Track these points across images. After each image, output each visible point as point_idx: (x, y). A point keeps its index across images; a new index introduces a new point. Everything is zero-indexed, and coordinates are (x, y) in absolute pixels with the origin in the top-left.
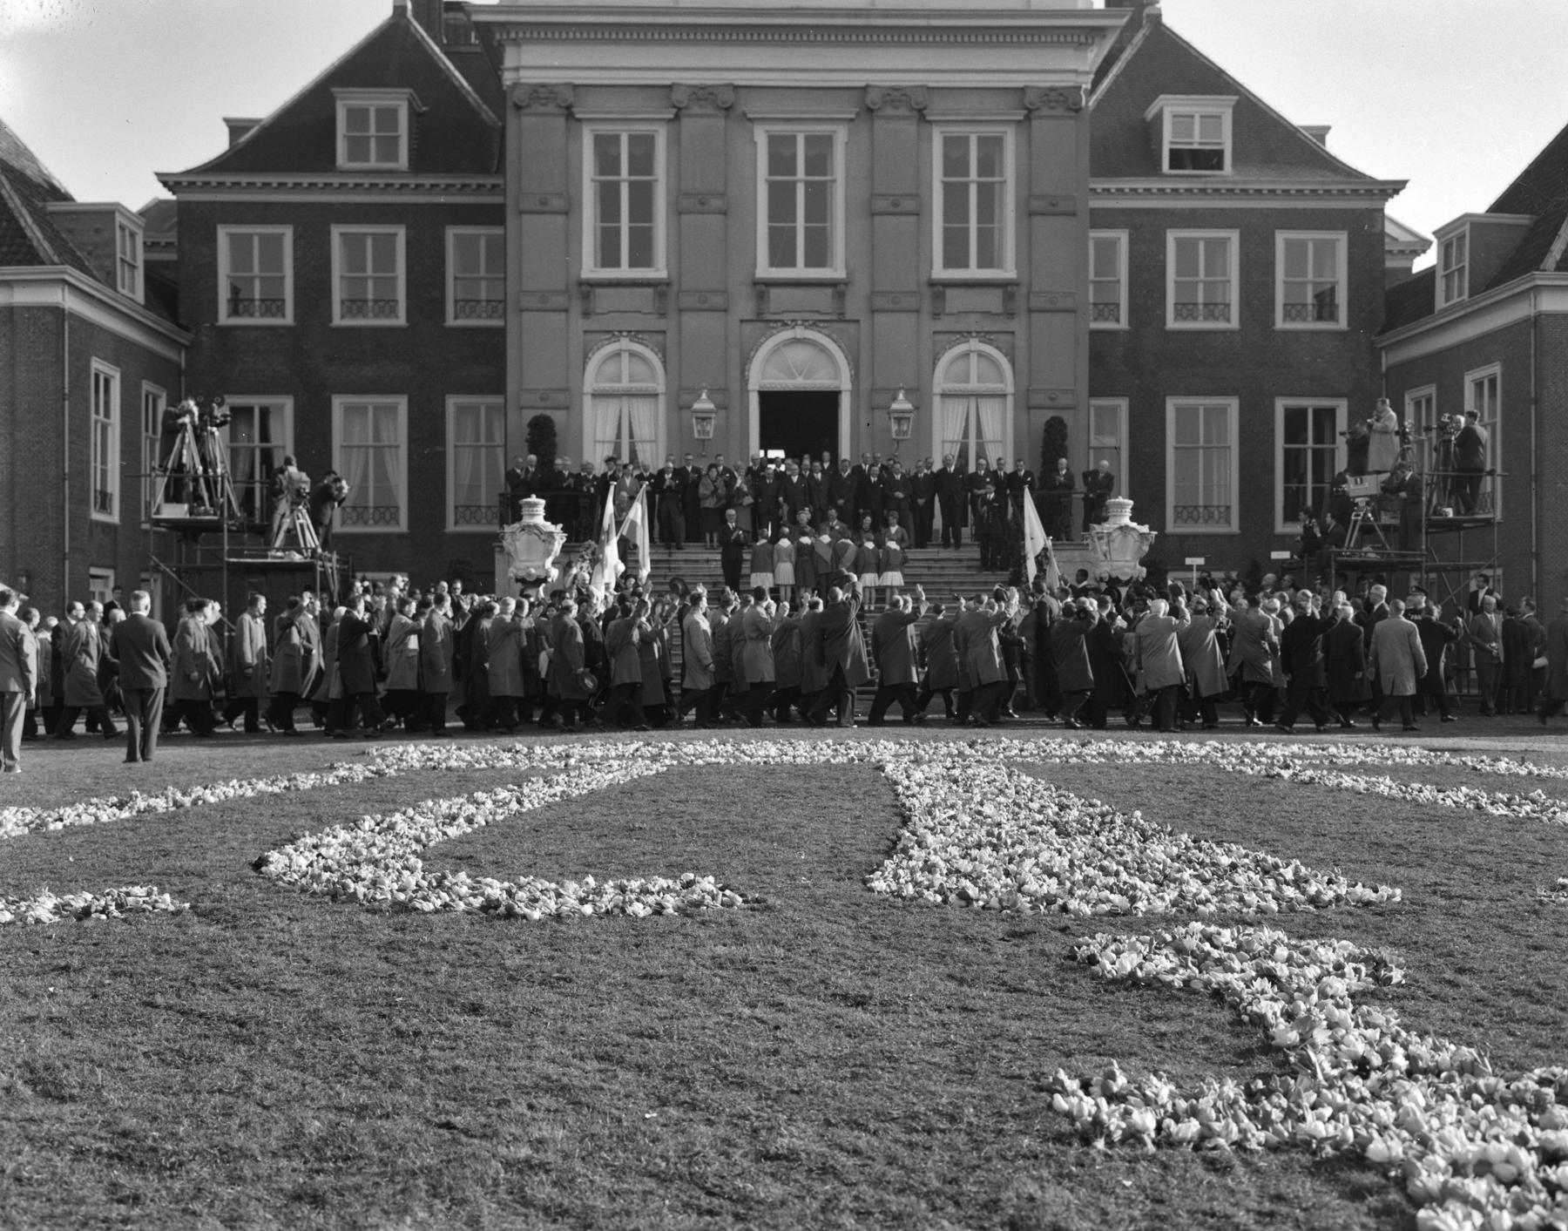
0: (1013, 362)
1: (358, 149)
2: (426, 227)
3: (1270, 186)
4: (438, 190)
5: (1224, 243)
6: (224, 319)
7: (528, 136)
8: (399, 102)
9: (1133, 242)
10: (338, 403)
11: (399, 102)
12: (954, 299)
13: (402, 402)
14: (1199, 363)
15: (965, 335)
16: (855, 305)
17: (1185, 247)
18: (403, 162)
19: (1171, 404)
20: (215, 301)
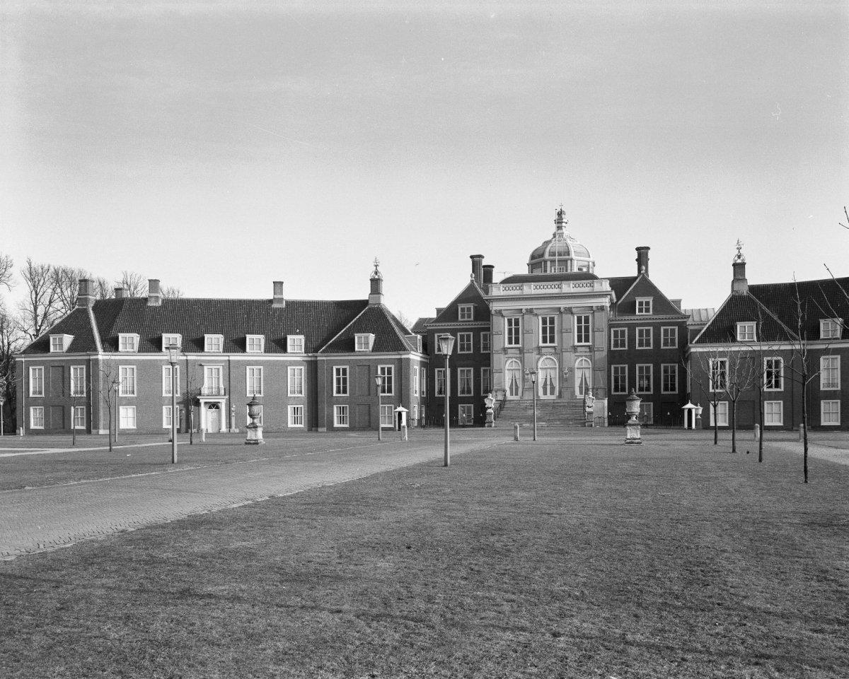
0: (591, 360)
1: (463, 316)
2: (477, 332)
3: (662, 317)
4: (479, 324)
5: (649, 330)
6: (436, 353)
7: (496, 320)
8: (471, 306)
9: (628, 330)
10: (459, 369)
11: (471, 306)
12: (579, 349)
13: (472, 369)
14: (643, 356)
15: (582, 356)
16: (558, 351)
17: (641, 332)
18: (472, 318)
19: (637, 366)
20: (434, 347)
